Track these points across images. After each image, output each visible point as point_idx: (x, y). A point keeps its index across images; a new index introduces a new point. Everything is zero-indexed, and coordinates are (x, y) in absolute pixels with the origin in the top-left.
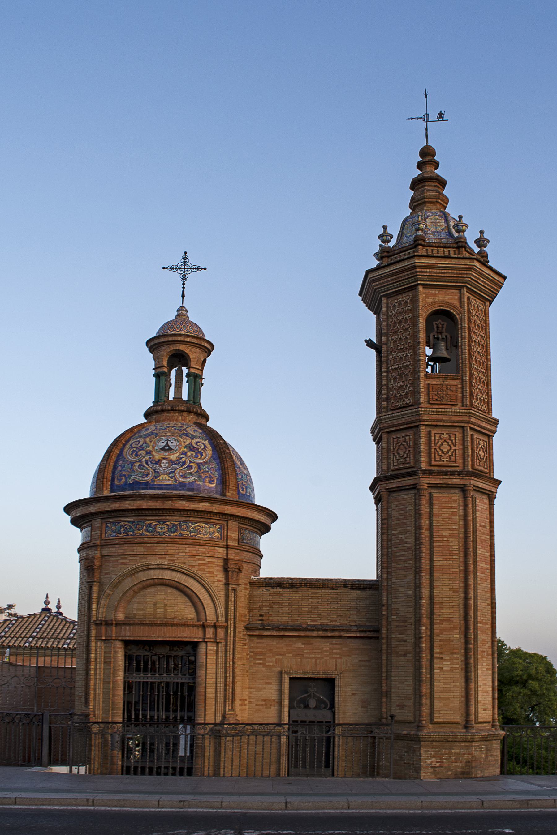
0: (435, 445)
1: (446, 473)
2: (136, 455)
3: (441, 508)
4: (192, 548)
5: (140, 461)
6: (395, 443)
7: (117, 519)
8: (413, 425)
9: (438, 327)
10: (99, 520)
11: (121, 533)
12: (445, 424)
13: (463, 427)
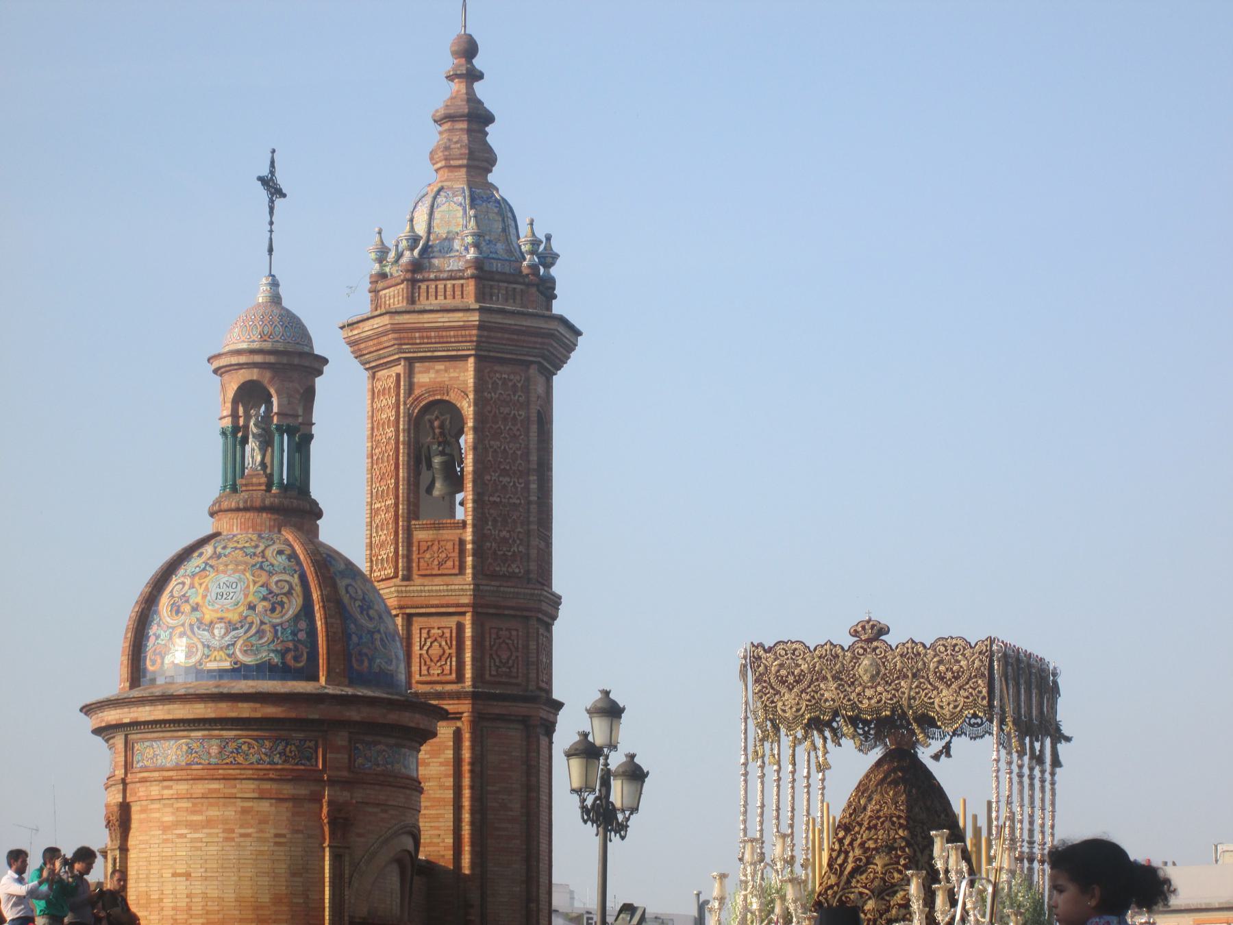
5: (379, 631)
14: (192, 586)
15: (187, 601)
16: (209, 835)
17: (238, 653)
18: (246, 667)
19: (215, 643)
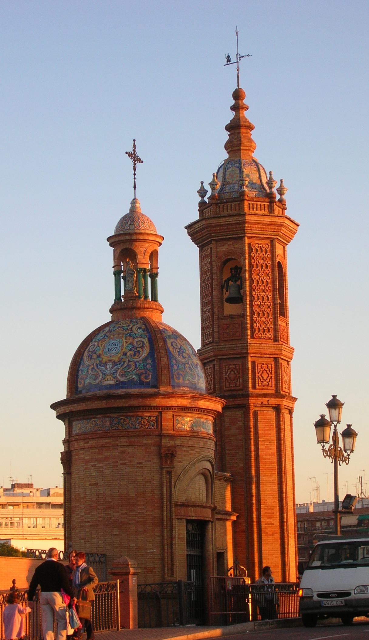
5: (188, 363)
14: (98, 346)
15: (95, 353)
16: (106, 465)
17: (118, 376)
18: (122, 383)
19: (107, 372)
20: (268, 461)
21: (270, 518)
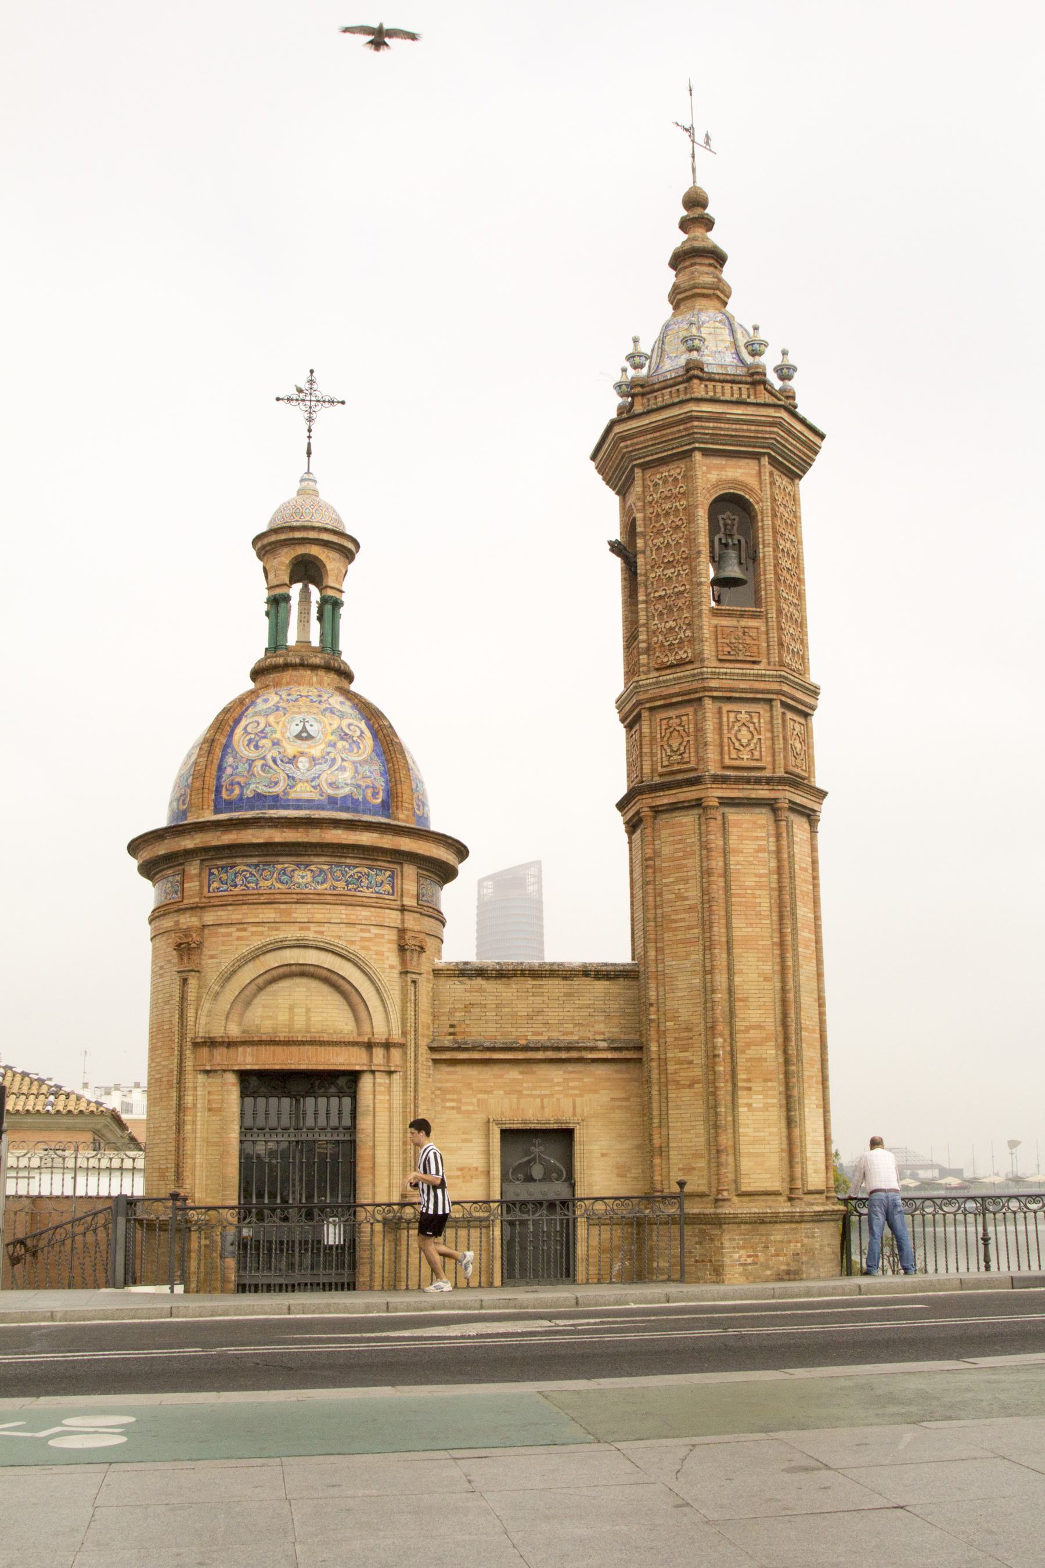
0: (729, 730)
1: (748, 781)
2: (257, 747)
3: (741, 838)
4: (350, 910)
5: (264, 758)
6: (664, 727)
7: (230, 861)
8: (693, 696)
9: (725, 525)
10: (196, 863)
11: (236, 886)
12: (743, 695)
13: (770, 701)
20: (683, 924)
21: (684, 1049)
